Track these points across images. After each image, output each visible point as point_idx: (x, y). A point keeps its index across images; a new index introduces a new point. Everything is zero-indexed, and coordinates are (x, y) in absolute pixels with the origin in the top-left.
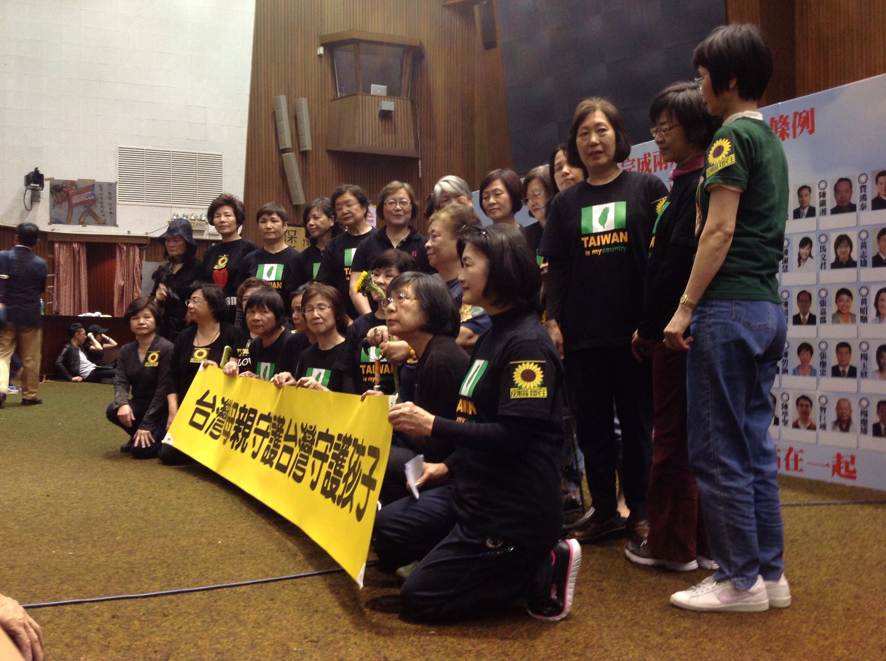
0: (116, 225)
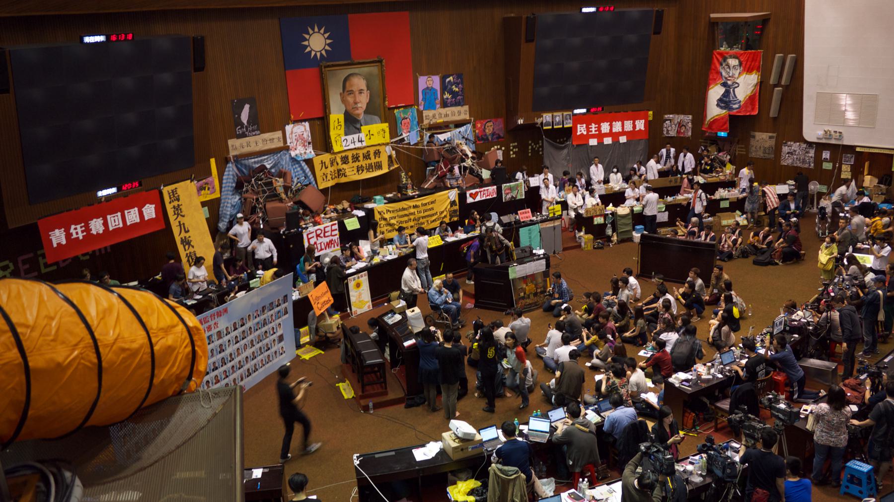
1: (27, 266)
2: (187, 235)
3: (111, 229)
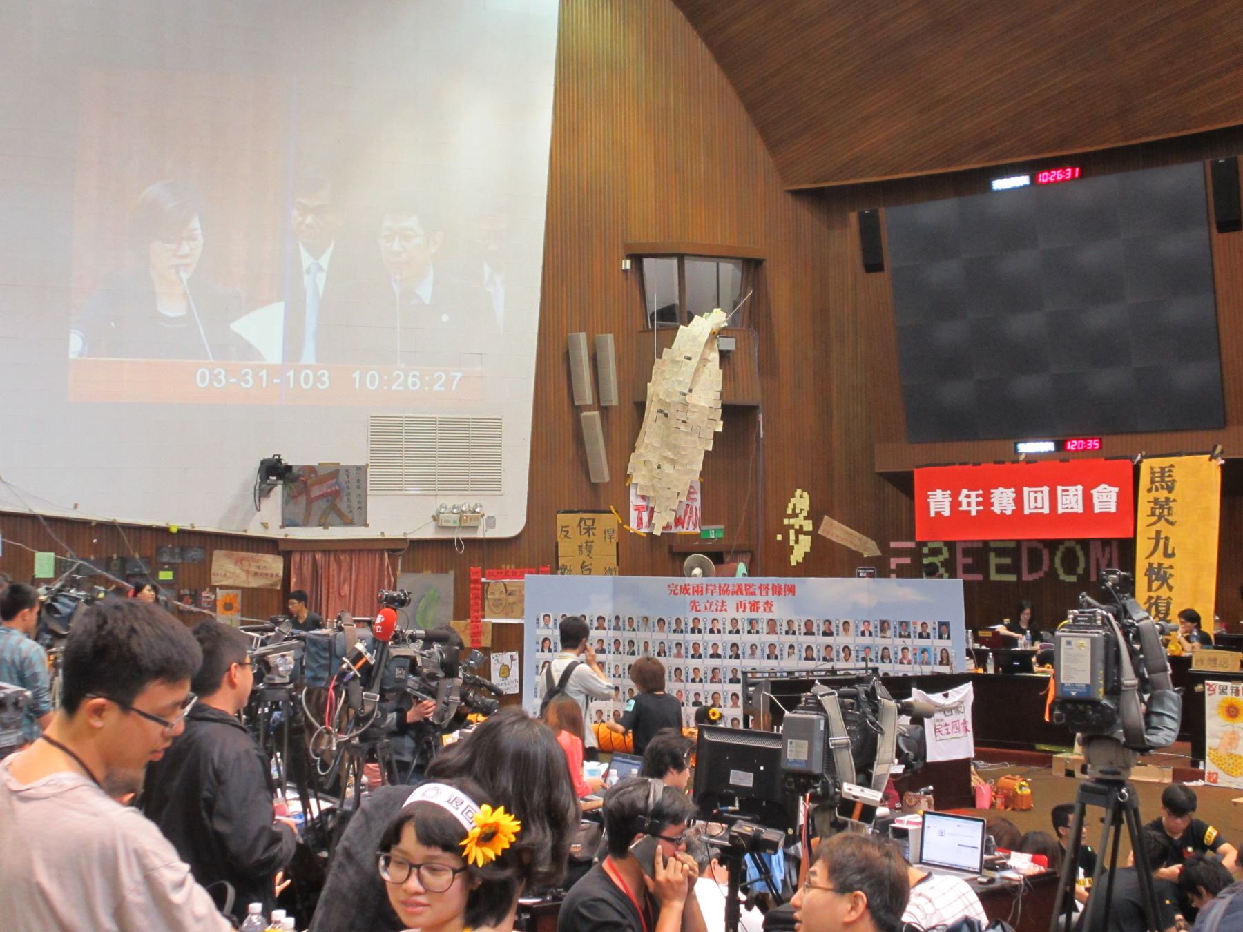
0: (366, 525)
1: (969, 561)
2: (1167, 562)
3: (1027, 512)
